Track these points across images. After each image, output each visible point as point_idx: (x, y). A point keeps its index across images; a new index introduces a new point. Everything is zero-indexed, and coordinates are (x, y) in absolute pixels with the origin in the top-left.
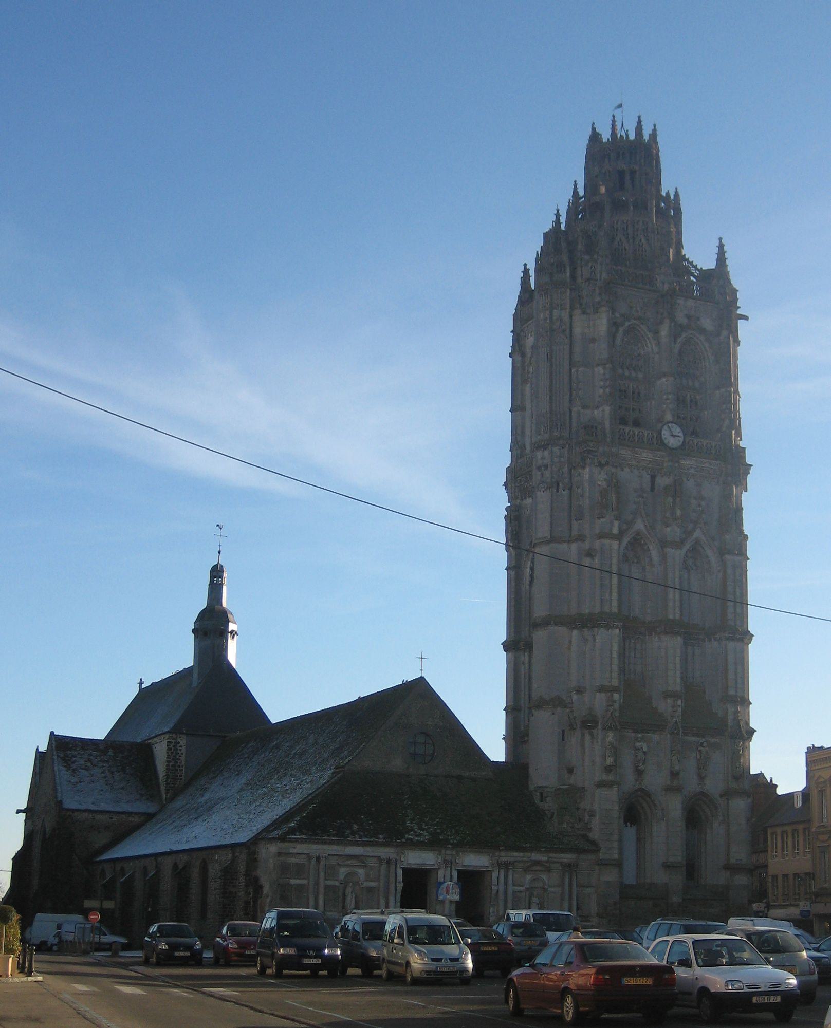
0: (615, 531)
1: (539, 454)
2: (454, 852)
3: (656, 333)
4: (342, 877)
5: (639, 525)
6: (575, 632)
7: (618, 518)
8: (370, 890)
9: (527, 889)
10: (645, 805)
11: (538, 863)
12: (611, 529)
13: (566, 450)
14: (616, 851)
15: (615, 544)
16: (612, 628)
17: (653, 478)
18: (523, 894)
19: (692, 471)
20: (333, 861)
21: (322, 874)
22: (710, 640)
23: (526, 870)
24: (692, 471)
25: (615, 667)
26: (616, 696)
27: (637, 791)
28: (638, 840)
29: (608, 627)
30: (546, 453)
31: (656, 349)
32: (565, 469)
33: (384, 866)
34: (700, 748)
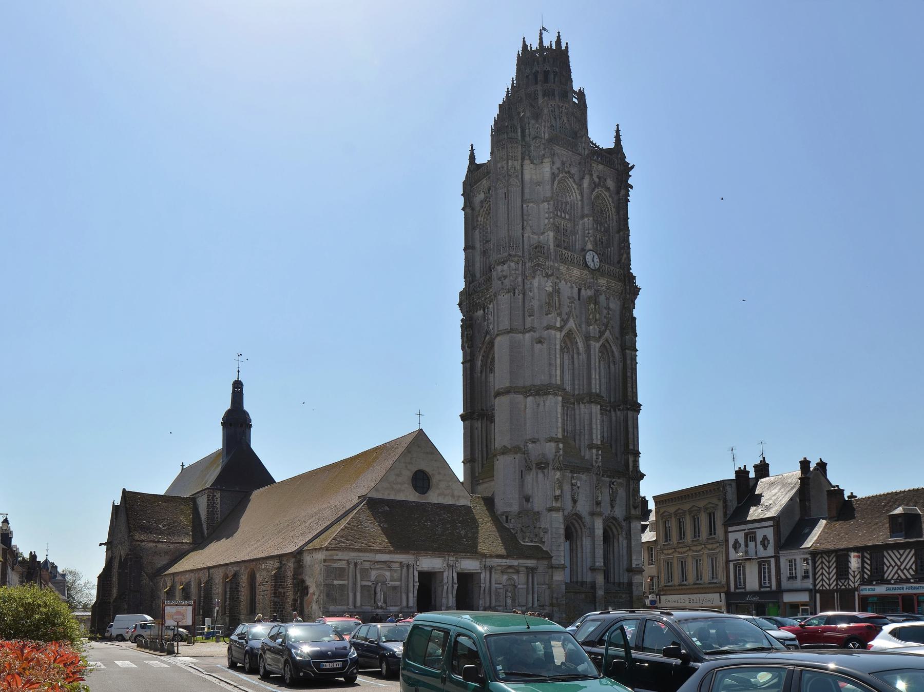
0: (558, 325)
1: (499, 268)
3: (580, 186)
5: (571, 324)
6: (530, 399)
8: (394, 588)
9: (504, 586)
11: (511, 567)
13: (520, 265)
17: (580, 290)
20: (367, 565)
28: (571, 550)
30: (505, 267)
31: (579, 198)
32: (520, 279)
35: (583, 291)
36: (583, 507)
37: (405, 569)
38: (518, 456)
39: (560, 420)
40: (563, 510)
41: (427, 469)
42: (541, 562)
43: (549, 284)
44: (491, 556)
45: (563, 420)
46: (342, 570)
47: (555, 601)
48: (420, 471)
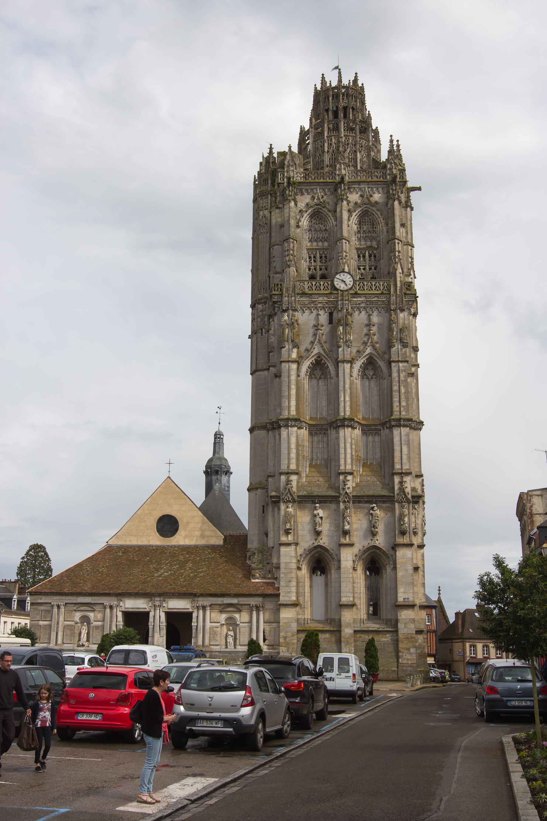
0: (294, 355)
2: (162, 599)
7: (296, 346)
8: (97, 627)
10: (326, 558)
12: (289, 356)
14: (295, 594)
15: (294, 366)
16: (291, 426)
17: (331, 314)
18: (219, 629)
21: (61, 619)
22: (384, 429)
23: (221, 612)
25: (293, 455)
26: (294, 478)
29: (287, 426)
31: (335, 223)
32: (266, 318)
34: (371, 512)
35: (335, 315)
37: (108, 610)
38: (259, 491)
40: (297, 544)
41: (173, 514)
44: (202, 595)
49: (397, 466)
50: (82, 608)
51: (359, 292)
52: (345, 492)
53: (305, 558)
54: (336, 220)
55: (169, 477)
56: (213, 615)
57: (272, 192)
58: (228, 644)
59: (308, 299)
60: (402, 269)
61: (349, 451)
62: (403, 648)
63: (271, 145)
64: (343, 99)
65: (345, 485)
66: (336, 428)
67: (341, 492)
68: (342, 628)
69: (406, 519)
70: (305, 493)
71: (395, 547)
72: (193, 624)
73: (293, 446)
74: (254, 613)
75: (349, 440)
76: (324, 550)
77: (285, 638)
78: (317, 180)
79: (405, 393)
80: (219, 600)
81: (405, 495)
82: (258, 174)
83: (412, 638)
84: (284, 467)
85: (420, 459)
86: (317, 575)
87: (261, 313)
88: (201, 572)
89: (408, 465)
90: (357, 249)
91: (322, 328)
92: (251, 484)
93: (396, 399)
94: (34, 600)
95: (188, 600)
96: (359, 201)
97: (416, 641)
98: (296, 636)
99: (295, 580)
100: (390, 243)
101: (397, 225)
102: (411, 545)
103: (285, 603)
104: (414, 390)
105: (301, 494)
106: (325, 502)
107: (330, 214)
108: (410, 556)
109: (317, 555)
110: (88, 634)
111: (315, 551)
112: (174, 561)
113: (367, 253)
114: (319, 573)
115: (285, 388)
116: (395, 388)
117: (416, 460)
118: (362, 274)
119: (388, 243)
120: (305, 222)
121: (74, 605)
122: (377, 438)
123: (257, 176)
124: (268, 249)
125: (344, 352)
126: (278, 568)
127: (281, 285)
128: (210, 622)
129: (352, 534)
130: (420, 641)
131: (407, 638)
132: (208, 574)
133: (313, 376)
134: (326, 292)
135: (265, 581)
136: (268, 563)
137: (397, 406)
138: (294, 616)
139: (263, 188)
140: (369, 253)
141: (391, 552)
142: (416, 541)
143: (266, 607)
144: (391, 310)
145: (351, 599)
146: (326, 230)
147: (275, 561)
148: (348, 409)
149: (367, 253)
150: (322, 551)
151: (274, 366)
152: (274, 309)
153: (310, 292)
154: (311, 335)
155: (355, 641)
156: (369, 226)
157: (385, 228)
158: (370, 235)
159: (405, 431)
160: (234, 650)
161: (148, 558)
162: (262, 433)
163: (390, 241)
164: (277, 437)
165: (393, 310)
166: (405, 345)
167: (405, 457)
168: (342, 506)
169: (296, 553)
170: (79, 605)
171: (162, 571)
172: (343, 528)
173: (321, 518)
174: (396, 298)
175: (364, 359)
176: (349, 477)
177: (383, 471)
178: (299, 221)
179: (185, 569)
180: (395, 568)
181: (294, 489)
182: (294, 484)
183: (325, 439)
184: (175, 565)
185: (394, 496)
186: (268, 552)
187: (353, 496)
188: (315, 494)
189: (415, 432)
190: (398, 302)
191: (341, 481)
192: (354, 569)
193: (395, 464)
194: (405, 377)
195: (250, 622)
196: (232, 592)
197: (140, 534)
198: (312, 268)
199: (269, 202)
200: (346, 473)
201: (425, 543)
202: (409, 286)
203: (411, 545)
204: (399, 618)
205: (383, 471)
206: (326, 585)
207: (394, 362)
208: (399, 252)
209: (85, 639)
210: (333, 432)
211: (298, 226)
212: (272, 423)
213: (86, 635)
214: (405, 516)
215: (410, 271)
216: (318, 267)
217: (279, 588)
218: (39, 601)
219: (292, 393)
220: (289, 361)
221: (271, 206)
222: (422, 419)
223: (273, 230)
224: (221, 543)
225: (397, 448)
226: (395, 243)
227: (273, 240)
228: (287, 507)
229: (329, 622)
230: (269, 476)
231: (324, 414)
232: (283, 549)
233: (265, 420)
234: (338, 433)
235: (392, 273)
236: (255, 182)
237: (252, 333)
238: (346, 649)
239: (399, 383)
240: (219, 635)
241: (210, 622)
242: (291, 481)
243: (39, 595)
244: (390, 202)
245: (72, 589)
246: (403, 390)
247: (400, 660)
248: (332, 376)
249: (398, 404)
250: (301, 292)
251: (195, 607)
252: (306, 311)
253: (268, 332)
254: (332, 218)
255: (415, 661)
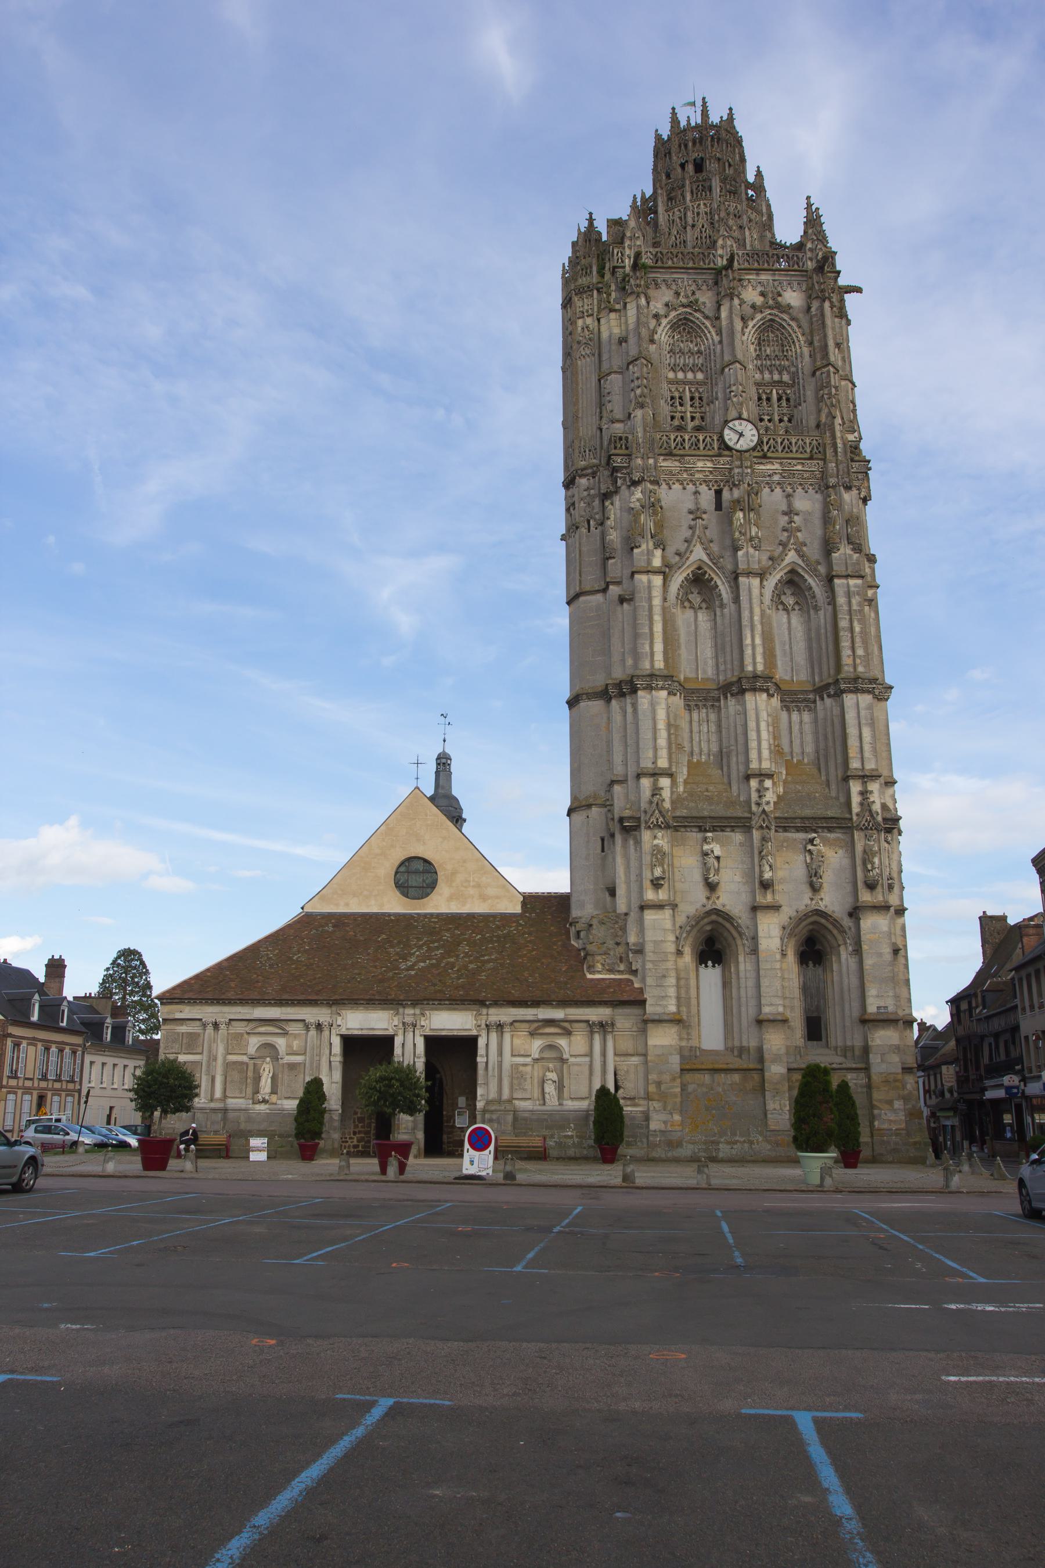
0: (657, 562)
2: (418, 1011)
4: (252, 1050)
7: (660, 544)
8: (292, 1066)
9: (536, 1060)
10: (726, 934)
12: (649, 562)
14: (673, 1001)
16: (657, 689)
17: (718, 493)
18: (529, 1069)
19: (776, 478)
22: (822, 699)
23: (532, 1034)
24: (776, 478)
25: (662, 742)
26: (665, 782)
27: (709, 913)
29: (649, 688)
31: (717, 338)
33: (313, 1032)
34: (810, 847)
35: (726, 495)
36: (732, 897)
39: (663, 735)
40: (674, 906)
42: (619, 1011)
43: (638, 495)
44: (496, 1003)
45: (669, 735)
46: (193, 1037)
47: (652, 1088)
48: (410, 859)
49: (855, 764)
50: (262, 1029)
51: (769, 454)
52: (761, 809)
53: (689, 933)
54: (719, 333)
55: (417, 788)
56: (517, 1042)
57: (600, 285)
58: (547, 1096)
59: (677, 464)
60: (842, 418)
61: (764, 735)
62: (880, 1101)
63: (591, 214)
64: (712, 146)
65: (760, 797)
66: (737, 694)
67: (754, 808)
68: (766, 1064)
69: (876, 860)
70: (684, 812)
71: (855, 913)
72: (479, 1059)
73: (661, 725)
74: (597, 1038)
75: (764, 715)
76: (724, 918)
77: (659, 1084)
78: (681, 264)
79: (861, 632)
80: (528, 1013)
81: (872, 815)
82: (570, 262)
83: (896, 1081)
84: (646, 764)
85: (890, 754)
86: (706, 966)
87: (585, 493)
88: (488, 961)
89: (873, 761)
90: (758, 384)
91: (704, 516)
92: (574, 798)
93: (845, 644)
94: (168, 1013)
95: (469, 1013)
96: (759, 303)
97: (904, 1087)
98: (679, 1081)
99: (673, 974)
100: (818, 373)
101: (831, 343)
102: (886, 908)
103: (656, 1017)
104: (873, 630)
105: (678, 814)
106: (722, 829)
107: (708, 323)
108: (885, 929)
109: (708, 928)
110: (274, 1078)
111: (706, 920)
112: (433, 942)
113: (774, 391)
114: (710, 963)
115: (643, 620)
116: (843, 624)
117: (884, 754)
118: (767, 429)
119: (814, 374)
120: (663, 335)
121: (246, 1023)
122: (807, 717)
123: (567, 264)
124: (594, 379)
125: (748, 556)
126: (640, 951)
127: (627, 438)
128: (512, 1055)
129: (776, 887)
130: (909, 1086)
131: (887, 1081)
132: (502, 965)
133: (686, 604)
134: (710, 453)
135: (612, 976)
136: (618, 944)
137: (849, 656)
138: (673, 1043)
139: (583, 281)
140: (778, 393)
141: (847, 922)
142: (893, 900)
143: (618, 1025)
144: (828, 487)
145: (781, 1009)
146: (699, 352)
147: (632, 939)
148: (759, 659)
149: (774, 391)
150: (720, 920)
151: (618, 583)
152: (615, 482)
153: (681, 452)
154: (685, 527)
155: (790, 1088)
156: (776, 348)
157: (806, 351)
158: (778, 363)
159: (865, 699)
160: (559, 1108)
161: (384, 936)
162: (595, 706)
163: (818, 369)
164: (629, 710)
165: (834, 487)
166: (859, 546)
167: (867, 747)
168: (756, 834)
169: (674, 924)
170: (257, 1023)
171: (413, 959)
172: (761, 876)
173: (718, 858)
174: (837, 466)
175: (782, 573)
176: (768, 783)
177: (823, 773)
178: (654, 332)
179: (457, 956)
180: (858, 951)
181: (667, 805)
182: (666, 794)
183: (713, 717)
184: (437, 948)
185: (851, 819)
186: (617, 922)
187: (776, 818)
188: (706, 814)
189: (882, 704)
190: (841, 473)
191: (753, 789)
192: (784, 955)
193: (851, 761)
194: (860, 604)
195: (590, 1054)
196: (553, 997)
197: (365, 893)
198: (678, 415)
199: (595, 301)
200: (762, 775)
201: (906, 905)
202: (855, 449)
203: (886, 908)
204: (870, 1043)
205: (823, 773)
206: (726, 984)
207: (839, 577)
208: (836, 388)
209: (268, 1089)
210: (732, 702)
211: (652, 341)
212: (619, 685)
213: (269, 1080)
214: (874, 854)
215: (852, 426)
216: (689, 415)
217: (641, 991)
218: (178, 1016)
219: (655, 629)
220: (648, 572)
221: (599, 308)
222: (889, 680)
223: (605, 349)
224: (518, 909)
225: (852, 731)
226: (829, 372)
227: (605, 366)
228: (655, 837)
229: (736, 1053)
230: (613, 782)
231: (710, 672)
232: (650, 916)
233: (599, 681)
234: (744, 704)
235: (825, 424)
236: (563, 275)
237: (568, 529)
238: (774, 1103)
239: (851, 615)
240: (529, 1081)
241: (512, 1055)
242: (662, 789)
243: (177, 1003)
244: (815, 305)
245: (242, 993)
246: (857, 628)
247: (876, 1123)
248: (725, 601)
249: (849, 652)
250: (664, 452)
251: (483, 1026)
252: (674, 487)
253: (602, 524)
254: (711, 330)
255: (903, 1126)
